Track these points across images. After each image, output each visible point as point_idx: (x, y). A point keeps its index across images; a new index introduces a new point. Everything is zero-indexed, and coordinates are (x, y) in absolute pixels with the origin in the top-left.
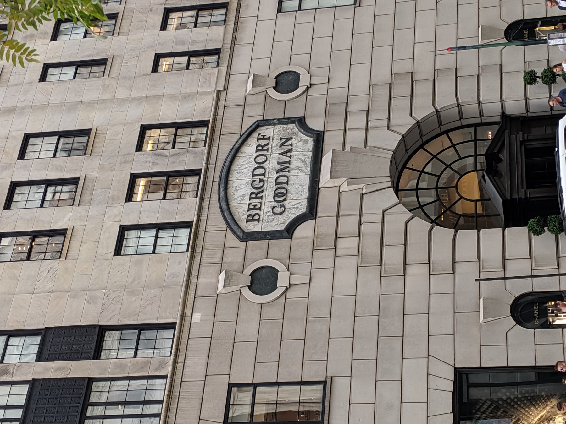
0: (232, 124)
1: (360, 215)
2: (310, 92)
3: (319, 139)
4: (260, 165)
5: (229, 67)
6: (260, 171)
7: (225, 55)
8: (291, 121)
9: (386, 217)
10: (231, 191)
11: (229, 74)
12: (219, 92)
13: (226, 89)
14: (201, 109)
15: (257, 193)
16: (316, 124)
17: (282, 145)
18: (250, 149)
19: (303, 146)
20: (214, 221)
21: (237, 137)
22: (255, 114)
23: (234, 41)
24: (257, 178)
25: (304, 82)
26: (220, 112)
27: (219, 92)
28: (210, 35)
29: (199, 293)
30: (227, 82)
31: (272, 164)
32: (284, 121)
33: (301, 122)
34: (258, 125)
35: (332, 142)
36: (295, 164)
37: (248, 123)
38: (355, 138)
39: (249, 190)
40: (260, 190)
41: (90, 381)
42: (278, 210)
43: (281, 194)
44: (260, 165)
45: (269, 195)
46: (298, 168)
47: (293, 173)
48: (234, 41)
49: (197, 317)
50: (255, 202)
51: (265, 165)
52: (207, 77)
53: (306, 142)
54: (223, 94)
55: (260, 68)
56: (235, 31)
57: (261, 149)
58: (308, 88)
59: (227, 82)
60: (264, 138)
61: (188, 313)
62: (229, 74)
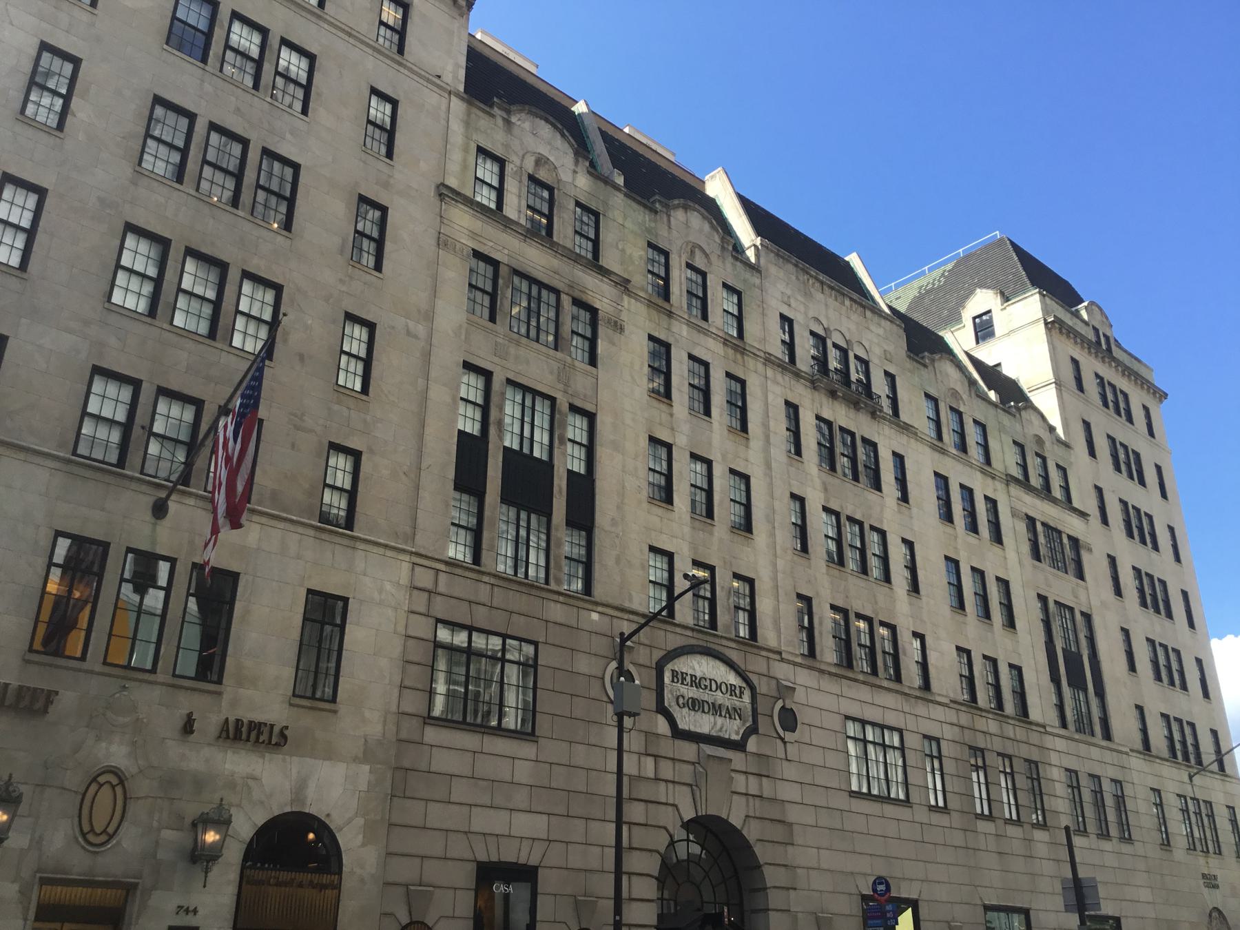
0: (756, 664)
1: (673, 782)
2: (778, 741)
3: (739, 746)
4: (719, 687)
5: (800, 665)
6: (714, 687)
7: (809, 662)
8: (755, 721)
9: (670, 808)
10: (698, 657)
11: (795, 664)
12: (780, 653)
13: (782, 660)
14: (768, 636)
15: (696, 682)
16: (752, 745)
17: (735, 709)
18: (733, 679)
19: (732, 729)
20: (674, 640)
21: (743, 667)
22: (763, 687)
23: (822, 672)
24: (708, 683)
25: (788, 736)
26: (764, 653)
27: (780, 653)
28: (828, 651)
29: (615, 620)
30: (789, 662)
31: (720, 698)
32: (754, 710)
33: (753, 730)
34: (752, 688)
35: (737, 758)
36: (720, 721)
37: (754, 679)
38: (740, 783)
39: (699, 675)
40: (698, 686)
41: (549, 515)
42: (681, 700)
43: (695, 705)
44: (719, 687)
45: (692, 692)
46: (715, 724)
47: (712, 718)
48: (822, 672)
49: (595, 616)
50: (688, 679)
51: (718, 692)
52: (793, 644)
53: (737, 733)
54: (777, 657)
55: (800, 695)
56: (830, 674)
57: (732, 689)
58: (782, 739)
59: (789, 662)
60: (741, 693)
61: (600, 609)
62: (795, 664)
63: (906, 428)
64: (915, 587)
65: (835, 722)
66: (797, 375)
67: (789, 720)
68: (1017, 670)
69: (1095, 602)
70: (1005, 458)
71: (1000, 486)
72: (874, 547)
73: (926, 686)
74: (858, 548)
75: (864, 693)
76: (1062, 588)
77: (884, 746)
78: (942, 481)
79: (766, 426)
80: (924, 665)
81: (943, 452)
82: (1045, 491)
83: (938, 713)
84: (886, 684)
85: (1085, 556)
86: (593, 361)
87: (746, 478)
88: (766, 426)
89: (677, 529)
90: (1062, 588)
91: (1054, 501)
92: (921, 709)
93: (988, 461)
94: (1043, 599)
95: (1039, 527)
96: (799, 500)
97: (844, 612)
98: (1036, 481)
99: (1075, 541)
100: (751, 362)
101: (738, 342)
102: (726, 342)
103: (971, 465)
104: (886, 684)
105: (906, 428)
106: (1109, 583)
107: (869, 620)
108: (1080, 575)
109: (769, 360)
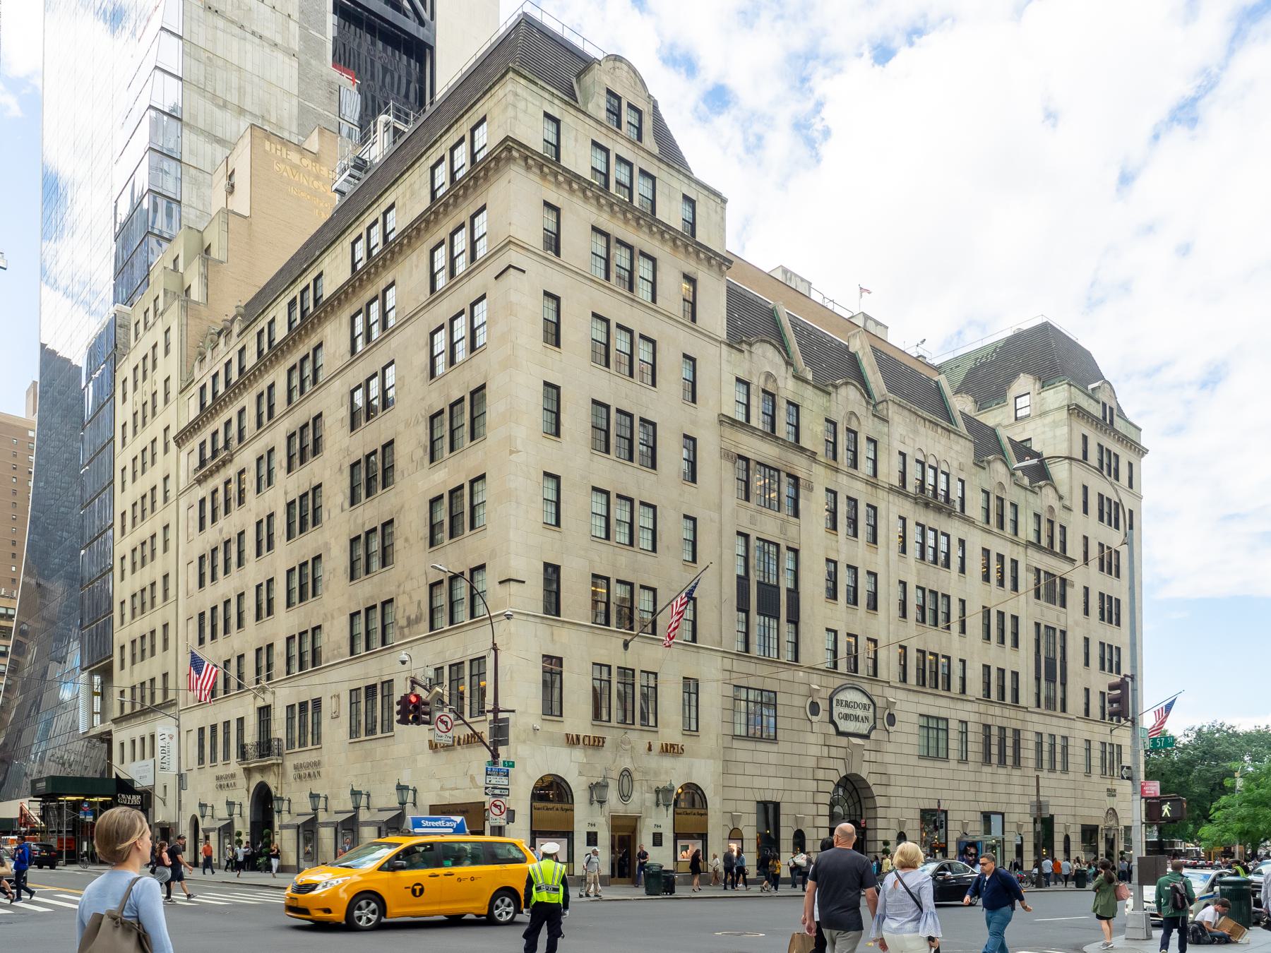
0: (875, 690)
16: (873, 736)
19: (863, 728)
20: (838, 682)
22: (880, 703)
25: (891, 729)
33: (874, 728)
63: (969, 521)
64: (963, 631)
65: (915, 718)
66: (907, 496)
67: (891, 719)
68: (1015, 675)
69: (1070, 622)
70: (1027, 530)
71: (1021, 549)
72: (942, 608)
73: (963, 691)
74: (934, 609)
75: (930, 700)
76: (1051, 615)
77: (938, 729)
78: (986, 552)
79: (888, 537)
80: (963, 679)
81: (990, 532)
82: (1050, 550)
83: (969, 706)
84: (943, 693)
85: (1069, 590)
86: (796, 514)
87: (875, 575)
88: (888, 537)
89: (840, 615)
90: (1051, 615)
91: (1055, 554)
92: (959, 705)
93: (1016, 534)
94: (1038, 625)
95: (1042, 574)
96: (903, 584)
97: (923, 652)
98: (1044, 543)
99: (1064, 581)
100: (882, 494)
101: (873, 481)
102: (867, 482)
103: (1005, 538)
104: (943, 693)
105: (969, 521)
106: (1082, 607)
107: (936, 655)
108: (1064, 605)
109: (891, 489)
